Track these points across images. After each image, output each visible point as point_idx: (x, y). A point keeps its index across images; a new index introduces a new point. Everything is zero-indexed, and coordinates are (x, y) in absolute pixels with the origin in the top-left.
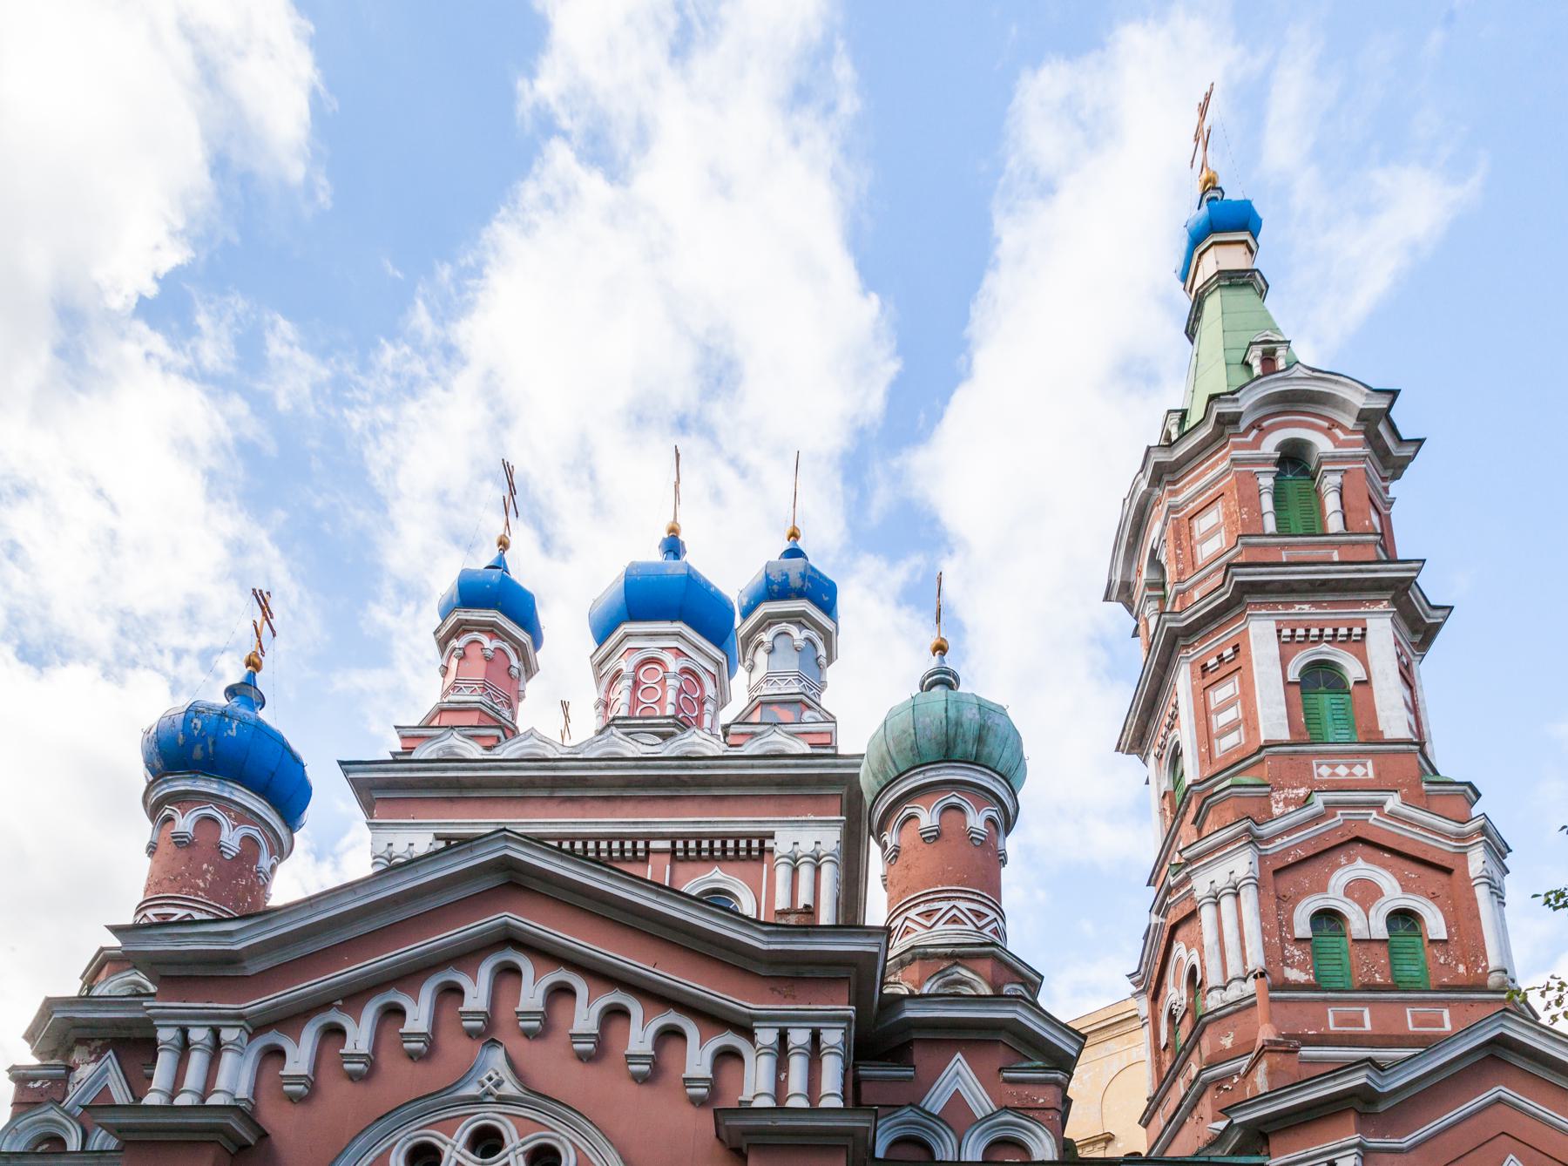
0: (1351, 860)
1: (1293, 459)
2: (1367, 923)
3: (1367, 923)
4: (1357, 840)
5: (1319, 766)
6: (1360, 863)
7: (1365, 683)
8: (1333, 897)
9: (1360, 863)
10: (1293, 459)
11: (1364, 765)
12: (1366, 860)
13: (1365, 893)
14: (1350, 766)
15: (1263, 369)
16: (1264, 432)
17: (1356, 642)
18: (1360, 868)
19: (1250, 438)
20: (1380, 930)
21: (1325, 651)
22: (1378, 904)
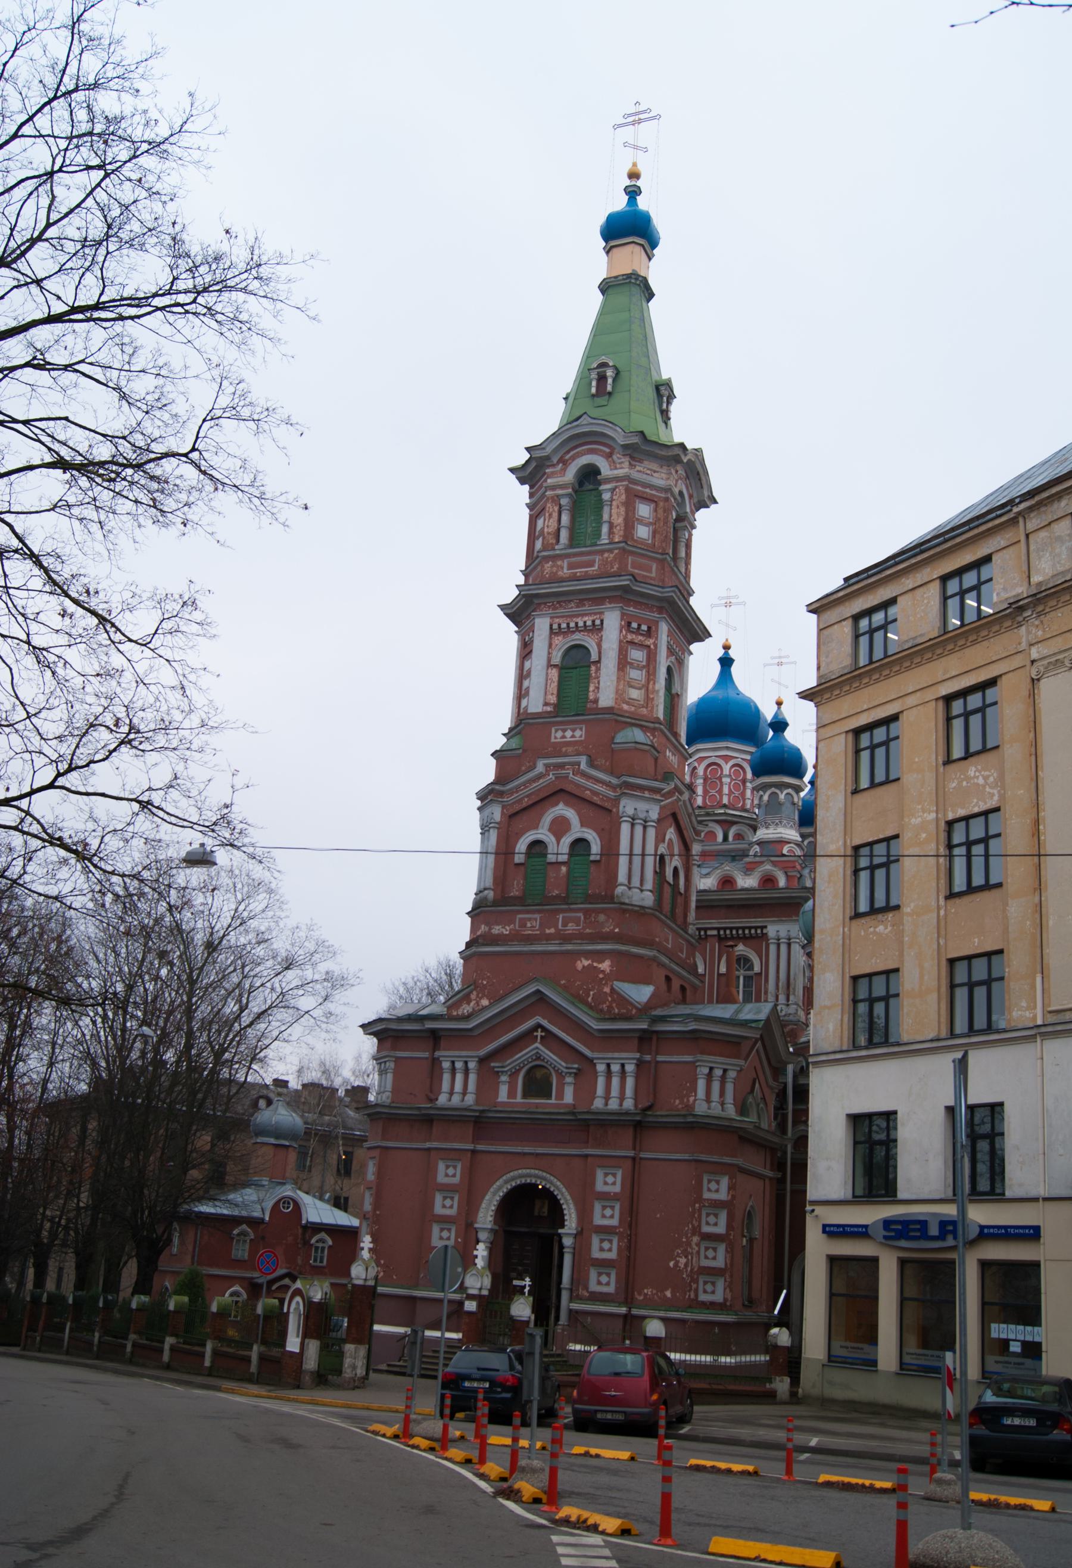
0: (557, 804)
1: (590, 474)
2: (559, 850)
3: (559, 850)
4: (562, 790)
5: (556, 731)
6: (561, 806)
7: (599, 662)
8: (542, 833)
10: (590, 474)
11: (581, 729)
12: (567, 804)
13: (560, 827)
14: (573, 730)
15: (597, 390)
16: (564, 462)
17: (596, 629)
21: (578, 638)
22: (568, 835)
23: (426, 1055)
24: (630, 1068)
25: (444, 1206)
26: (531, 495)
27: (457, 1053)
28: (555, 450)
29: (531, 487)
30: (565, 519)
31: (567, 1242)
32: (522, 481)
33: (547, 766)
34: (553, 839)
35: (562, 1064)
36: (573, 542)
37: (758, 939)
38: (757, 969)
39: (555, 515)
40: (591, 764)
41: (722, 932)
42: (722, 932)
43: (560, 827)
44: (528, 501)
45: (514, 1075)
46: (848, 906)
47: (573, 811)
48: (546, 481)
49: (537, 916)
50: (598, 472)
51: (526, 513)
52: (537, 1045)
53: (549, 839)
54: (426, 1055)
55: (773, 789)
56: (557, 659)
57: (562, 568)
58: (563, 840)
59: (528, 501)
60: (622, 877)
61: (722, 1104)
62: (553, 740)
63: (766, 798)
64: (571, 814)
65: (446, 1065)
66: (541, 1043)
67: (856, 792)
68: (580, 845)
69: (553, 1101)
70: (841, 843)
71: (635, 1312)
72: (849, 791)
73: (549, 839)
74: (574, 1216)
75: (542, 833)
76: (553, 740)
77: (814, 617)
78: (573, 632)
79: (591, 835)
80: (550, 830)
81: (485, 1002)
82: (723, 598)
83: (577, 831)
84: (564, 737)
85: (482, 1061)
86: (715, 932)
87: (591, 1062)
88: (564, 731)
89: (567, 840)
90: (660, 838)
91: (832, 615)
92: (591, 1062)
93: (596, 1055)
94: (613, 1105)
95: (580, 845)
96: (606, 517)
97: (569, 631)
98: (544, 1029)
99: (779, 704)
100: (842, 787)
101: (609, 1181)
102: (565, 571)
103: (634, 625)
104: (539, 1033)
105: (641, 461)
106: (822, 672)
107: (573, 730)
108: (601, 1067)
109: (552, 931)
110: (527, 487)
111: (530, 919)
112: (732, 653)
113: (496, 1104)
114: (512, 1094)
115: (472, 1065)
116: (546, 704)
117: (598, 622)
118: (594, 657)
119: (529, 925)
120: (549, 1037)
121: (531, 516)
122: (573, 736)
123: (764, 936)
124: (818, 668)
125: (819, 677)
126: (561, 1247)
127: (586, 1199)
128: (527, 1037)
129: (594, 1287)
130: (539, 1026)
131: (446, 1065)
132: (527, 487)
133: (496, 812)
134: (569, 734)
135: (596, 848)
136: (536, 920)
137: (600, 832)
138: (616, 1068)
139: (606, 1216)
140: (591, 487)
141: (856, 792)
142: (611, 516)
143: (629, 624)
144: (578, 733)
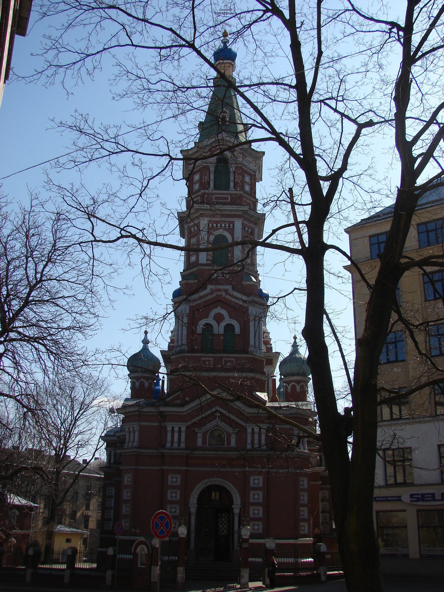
2: (219, 329)
3: (219, 329)
4: (219, 301)
6: (219, 308)
8: (210, 320)
9: (219, 308)
13: (219, 318)
18: (219, 310)
20: (222, 331)
23: (157, 424)
27: (176, 423)
30: (212, 177)
33: (212, 290)
34: (216, 323)
35: (229, 429)
36: (216, 188)
39: (208, 174)
40: (233, 289)
43: (219, 318)
45: (204, 435)
47: (225, 311)
49: (212, 359)
54: (157, 424)
57: (212, 199)
58: (221, 324)
60: (252, 342)
64: (224, 312)
65: (169, 429)
68: (229, 327)
74: (239, 499)
75: (210, 320)
78: (219, 229)
79: (234, 323)
80: (213, 319)
81: (187, 399)
83: (228, 320)
85: (187, 427)
89: (223, 324)
93: (248, 425)
95: (229, 327)
96: (232, 178)
97: (217, 229)
98: (220, 412)
102: (214, 200)
103: (246, 229)
104: (218, 414)
105: (246, 157)
108: (249, 430)
109: (220, 366)
111: (208, 361)
113: (196, 449)
114: (204, 442)
115: (183, 429)
116: (207, 260)
117: (231, 225)
119: (207, 363)
120: (223, 418)
126: (233, 514)
128: (212, 417)
130: (217, 411)
131: (169, 429)
133: (185, 308)
136: (211, 360)
137: (239, 322)
142: (234, 179)
143: (245, 227)
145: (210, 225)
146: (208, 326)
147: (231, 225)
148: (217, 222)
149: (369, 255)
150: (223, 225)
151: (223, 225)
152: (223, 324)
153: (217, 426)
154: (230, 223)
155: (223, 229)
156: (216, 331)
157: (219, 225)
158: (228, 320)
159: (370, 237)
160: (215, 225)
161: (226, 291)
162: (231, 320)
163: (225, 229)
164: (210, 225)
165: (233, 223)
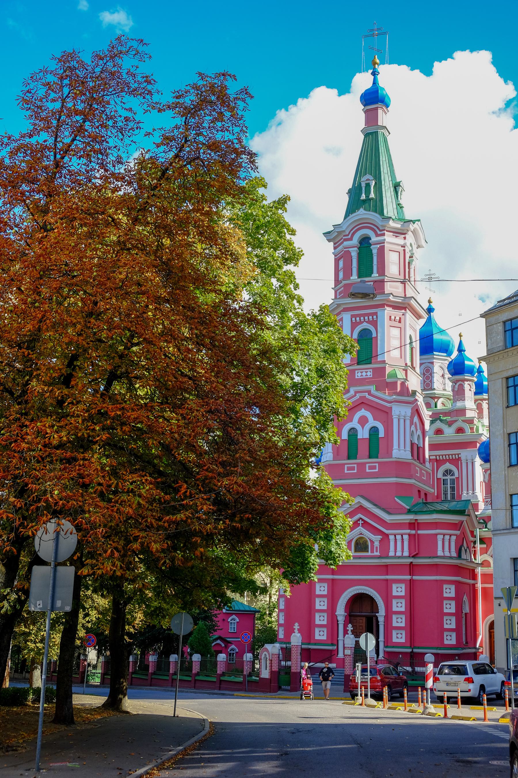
0: (361, 410)
1: (365, 241)
2: (363, 434)
3: (363, 434)
6: (363, 410)
9: (363, 410)
10: (365, 241)
13: (363, 421)
14: (366, 372)
18: (363, 412)
19: (349, 237)
20: (367, 436)
21: (365, 325)
24: (406, 537)
25: (321, 604)
26: (335, 248)
28: (346, 229)
29: (334, 244)
31: (381, 620)
32: (329, 241)
37: (456, 461)
38: (456, 475)
41: (438, 457)
42: (438, 457)
43: (363, 421)
44: (333, 251)
46: (506, 453)
48: (342, 243)
50: (370, 239)
51: (332, 259)
52: (360, 527)
53: (358, 427)
55: (460, 382)
56: (355, 336)
59: (333, 251)
61: (450, 552)
62: (356, 377)
63: (457, 386)
66: (362, 526)
67: (508, 407)
68: (374, 430)
69: (369, 554)
70: (502, 431)
71: (415, 650)
72: (505, 407)
73: (358, 427)
75: (355, 423)
76: (356, 377)
77: (484, 319)
78: (363, 322)
82: (427, 275)
84: (362, 376)
86: (434, 457)
87: (387, 535)
88: (362, 372)
89: (368, 427)
90: (412, 423)
91: (493, 319)
92: (387, 535)
94: (399, 554)
95: (374, 430)
97: (361, 322)
98: (363, 520)
99: (460, 336)
100: (501, 405)
101: (399, 590)
104: (361, 522)
106: (489, 347)
107: (366, 372)
108: (392, 537)
110: (332, 244)
112: (433, 305)
118: (374, 335)
120: (365, 524)
121: (335, 259)
122: (367, 375)
123: (459, 459)
124: (487, 346)
125: (488, 350)
126: (377, 622)
127: (388, 600)
129: (395, 640)
130: (361, 518)
132: (332, 244)
134: (364, 374)
135: (382, 434)
138: (399, 537)
139: (399, 606)
140: (366, 245)
141: (508, 407)
144: (369, 374)
145: (354, 319)
146: (353, 432)
147: (375, 317)
148: (360, 316)
149: (501, 344)
150: (366, 318)
151: (366, 318)
152: (368, 427)
153: (361, 534)
154: (373, 314)
155: (367, 322)
156: (360, 436)
157: (362, 318)
158: (372, 422)
159: (504, 322)
160: (358, 319)
161: (369, 392)
162: (376, 422)
163: (369, 322)
164: (354, 319)
165: (376, 314)
